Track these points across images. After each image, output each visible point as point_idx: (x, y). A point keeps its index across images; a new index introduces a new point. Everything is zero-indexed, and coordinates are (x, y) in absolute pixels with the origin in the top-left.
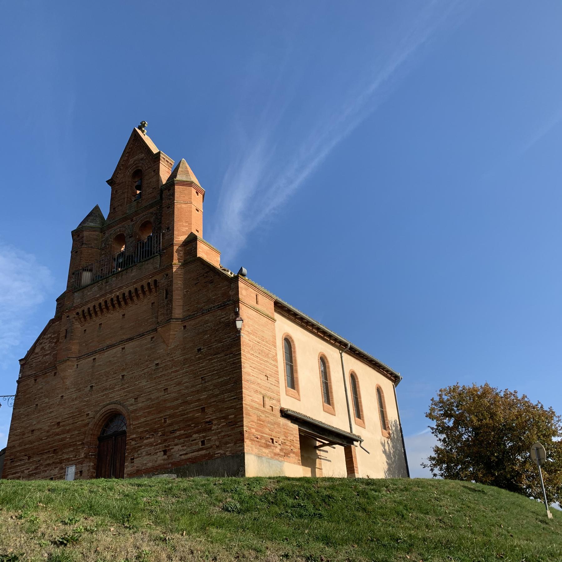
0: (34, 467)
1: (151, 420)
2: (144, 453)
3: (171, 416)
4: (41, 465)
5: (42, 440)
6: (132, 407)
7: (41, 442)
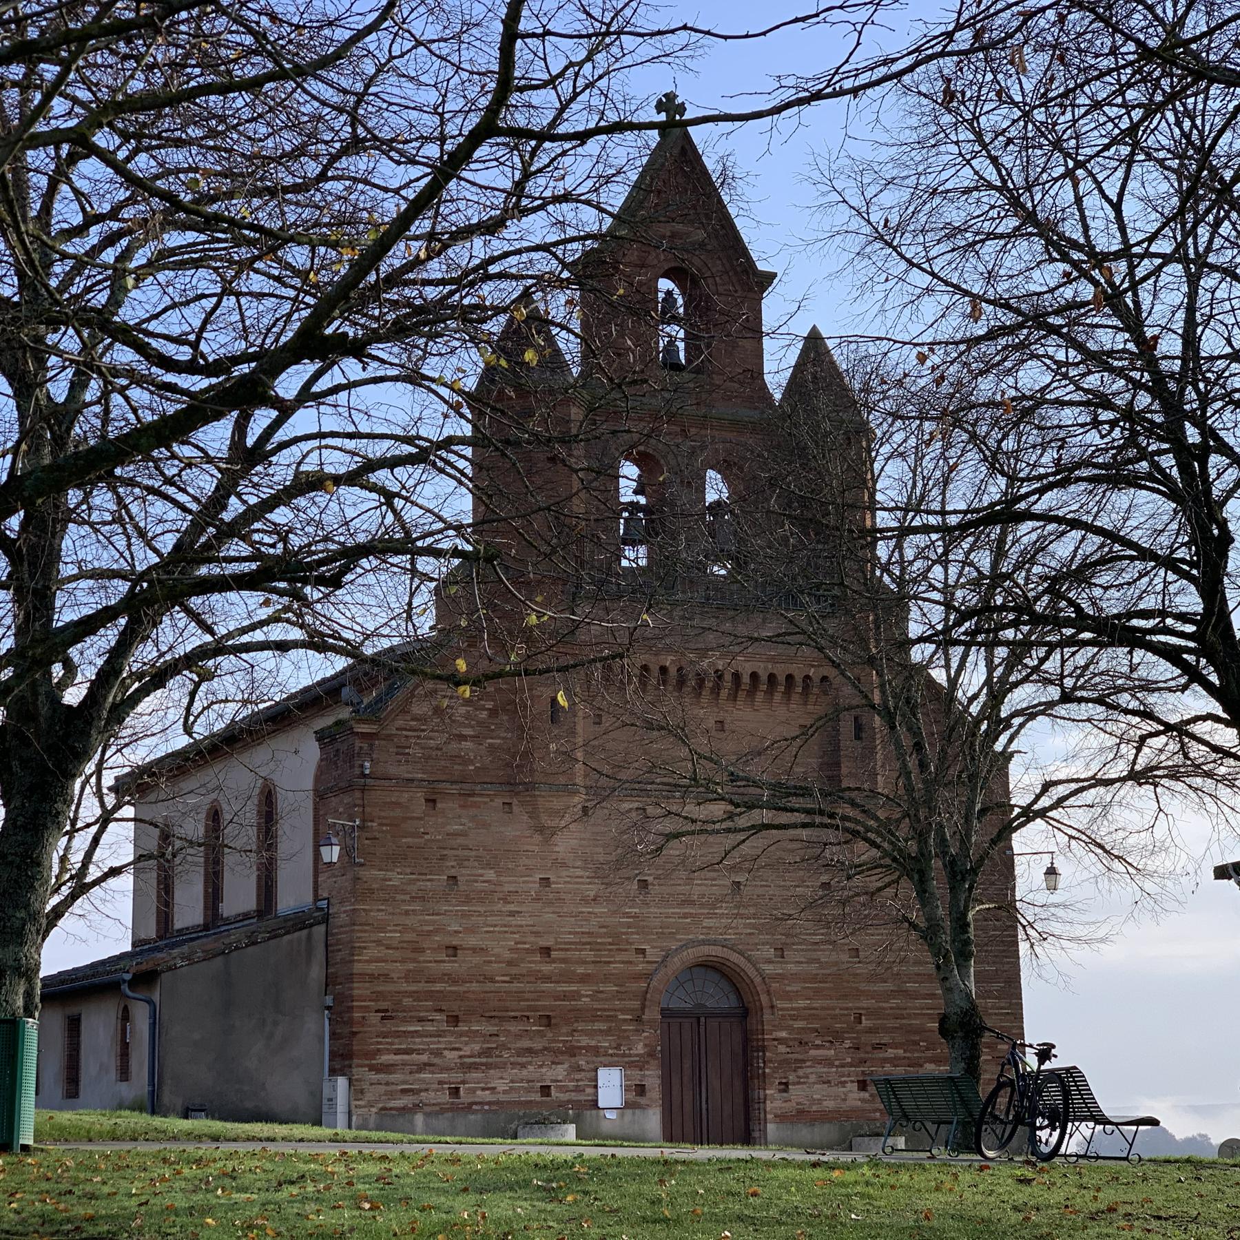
0: (477, 1047)
1: (823, 1008)
2: (813, 1078)
3: (872, 1013)
4: (504, 1047)
5: (492, 981)
6: (771, 967)
7: (489, 986)
